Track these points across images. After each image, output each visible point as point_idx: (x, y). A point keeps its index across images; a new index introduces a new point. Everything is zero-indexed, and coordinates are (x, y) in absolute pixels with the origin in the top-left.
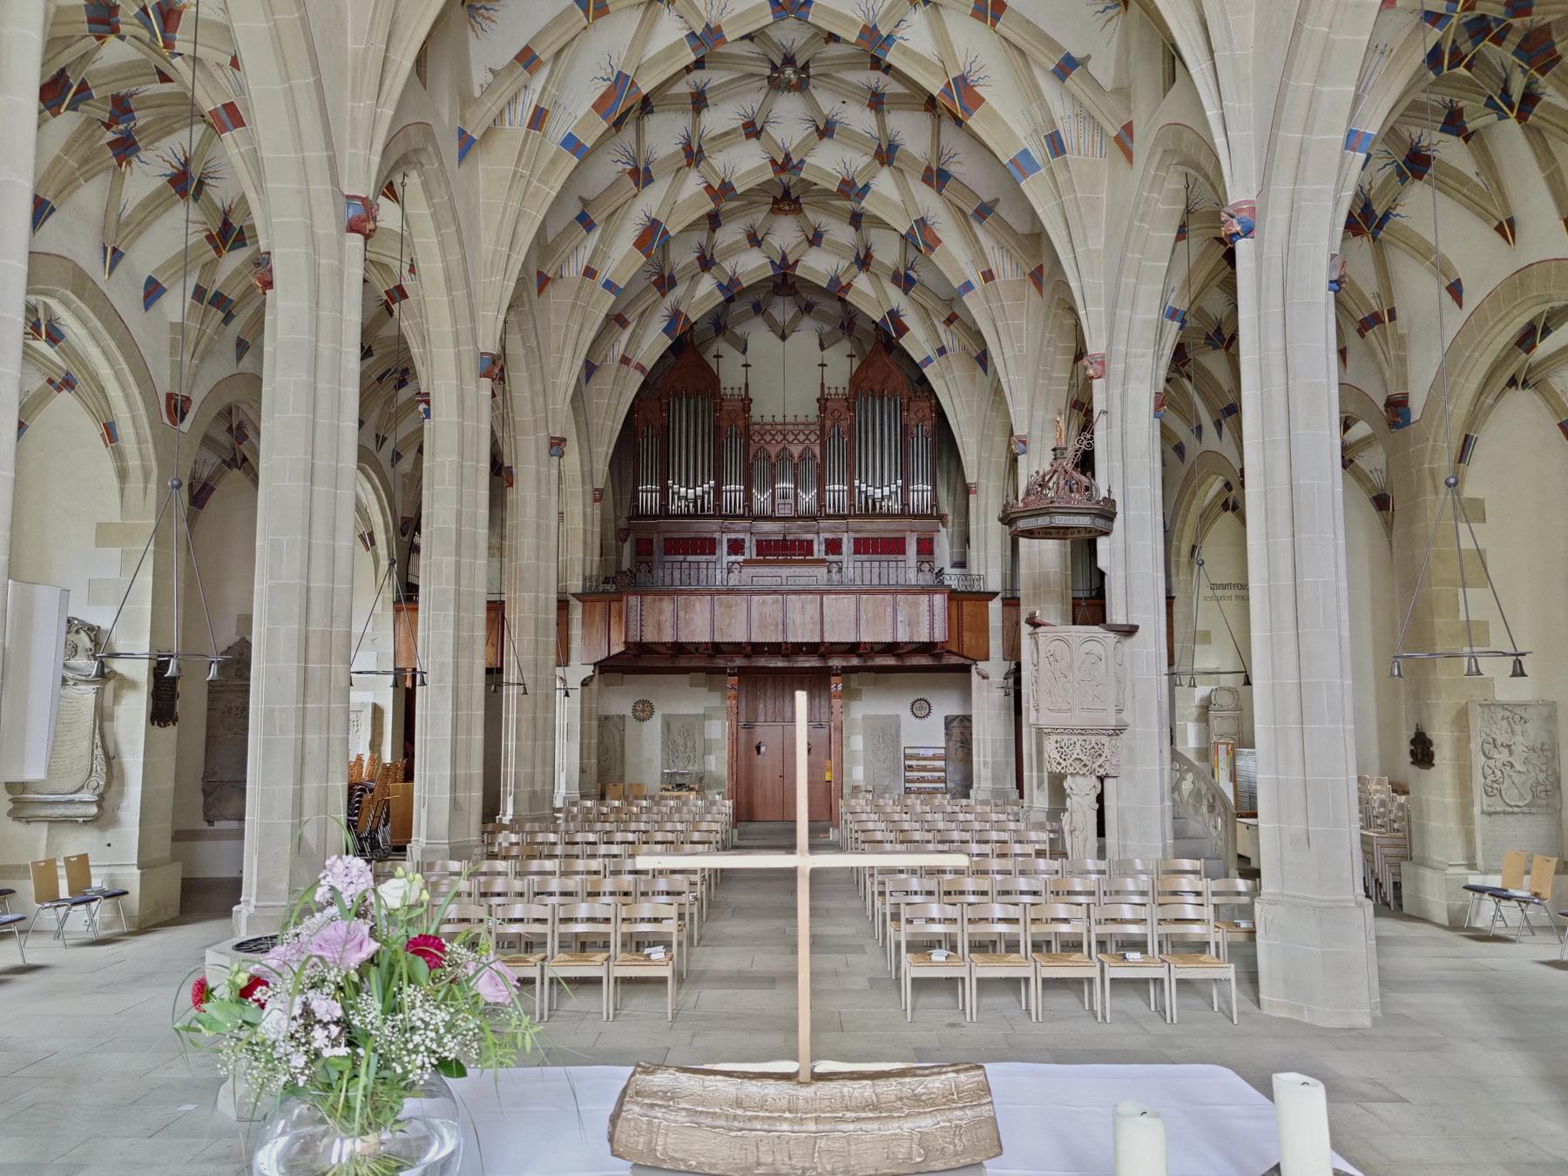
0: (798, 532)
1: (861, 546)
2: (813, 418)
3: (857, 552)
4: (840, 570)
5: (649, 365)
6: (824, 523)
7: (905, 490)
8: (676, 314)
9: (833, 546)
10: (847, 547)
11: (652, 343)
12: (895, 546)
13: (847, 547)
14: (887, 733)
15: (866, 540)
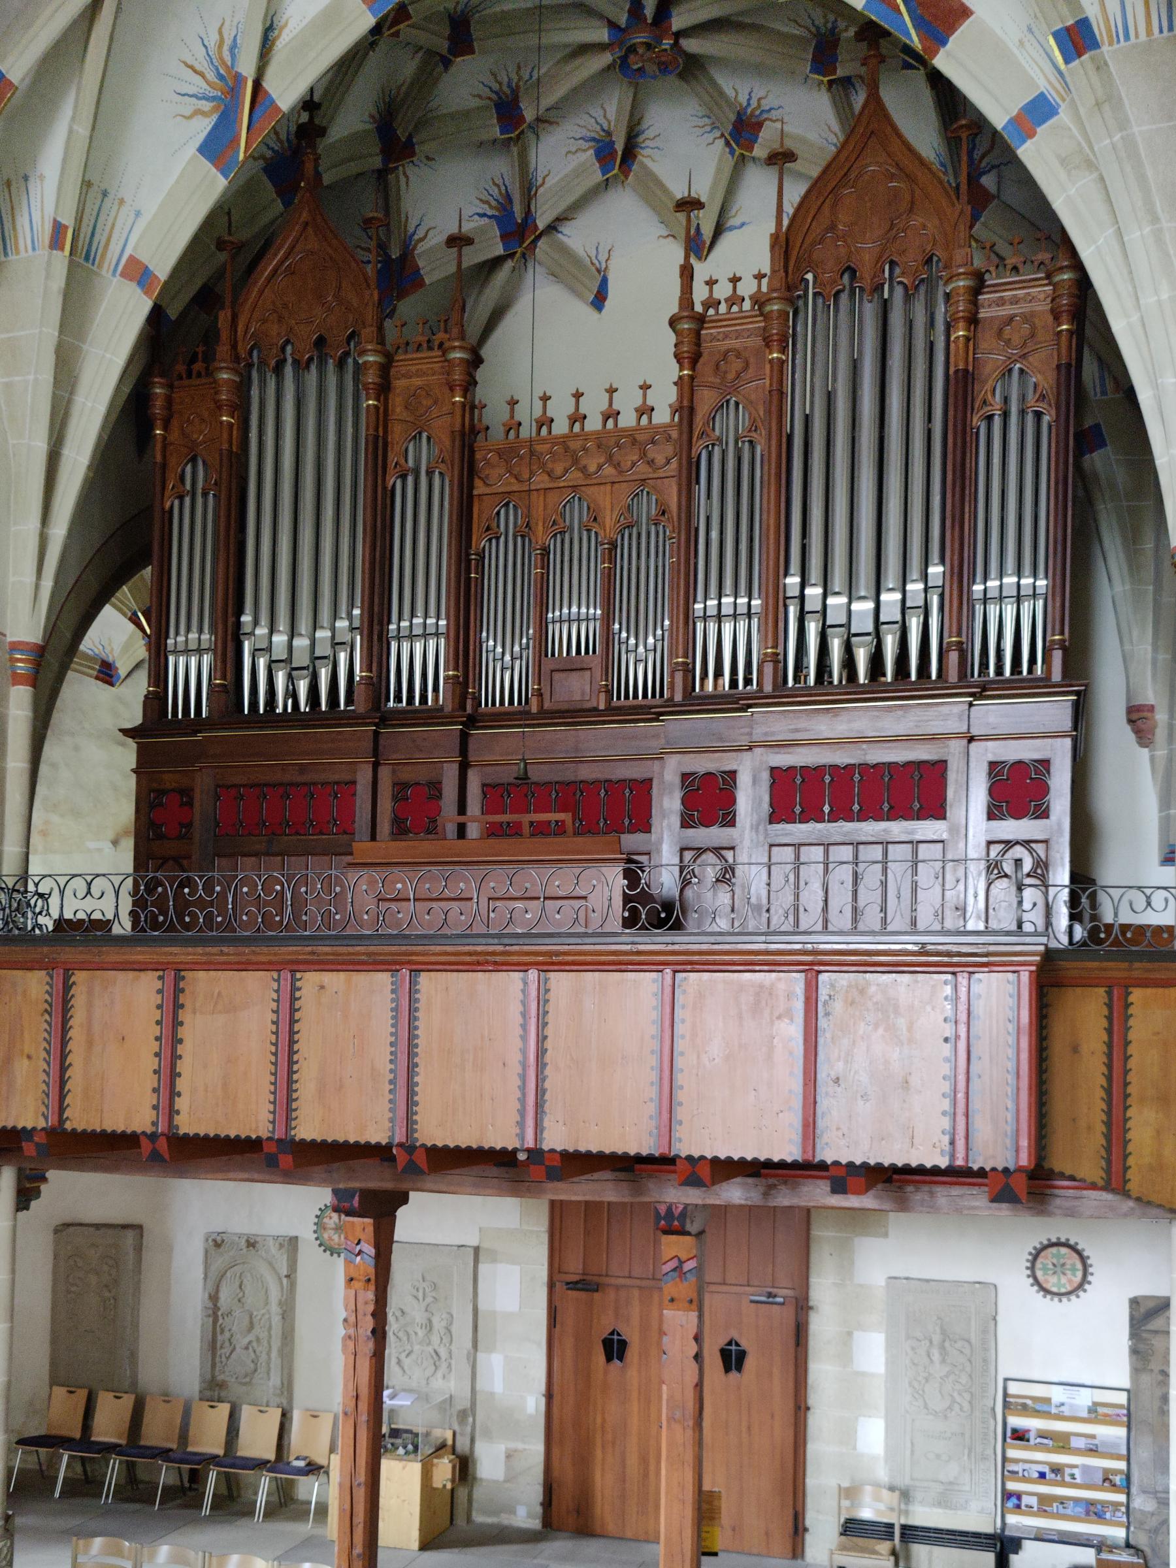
0: (602, 752)
1: (801, 795)
2: (664, 398)
3: (780, 812)
4: (726, 876)
5: (162, 268)
6: (678, 726)
7: (958, 596)
8: (241, 94)
9: (709, 800)
10: (751, 799)
11: (167, 191)
12: (916, 790)
13: (751, 799)
14: (955, 1337)
15: (812, 774)
